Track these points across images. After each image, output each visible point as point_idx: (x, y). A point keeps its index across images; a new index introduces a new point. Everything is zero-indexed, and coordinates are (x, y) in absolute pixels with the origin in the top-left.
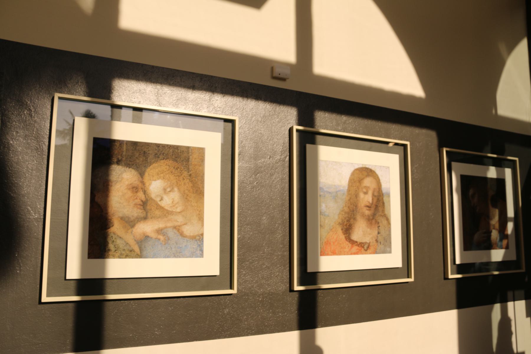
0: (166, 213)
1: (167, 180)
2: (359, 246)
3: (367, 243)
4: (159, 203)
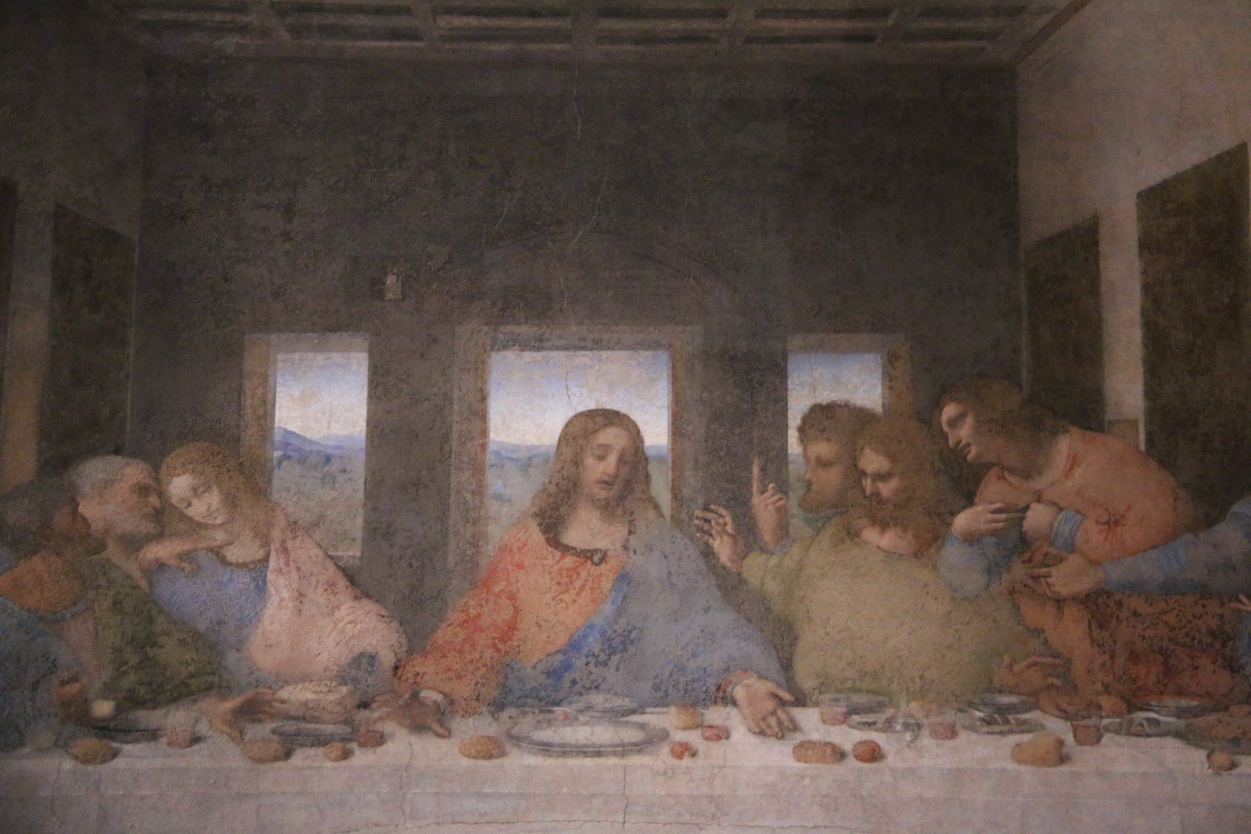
0: (196, 527)
1: (198, 474)
2: (579, 557)
3: (599, 552)
4: (185, 511)
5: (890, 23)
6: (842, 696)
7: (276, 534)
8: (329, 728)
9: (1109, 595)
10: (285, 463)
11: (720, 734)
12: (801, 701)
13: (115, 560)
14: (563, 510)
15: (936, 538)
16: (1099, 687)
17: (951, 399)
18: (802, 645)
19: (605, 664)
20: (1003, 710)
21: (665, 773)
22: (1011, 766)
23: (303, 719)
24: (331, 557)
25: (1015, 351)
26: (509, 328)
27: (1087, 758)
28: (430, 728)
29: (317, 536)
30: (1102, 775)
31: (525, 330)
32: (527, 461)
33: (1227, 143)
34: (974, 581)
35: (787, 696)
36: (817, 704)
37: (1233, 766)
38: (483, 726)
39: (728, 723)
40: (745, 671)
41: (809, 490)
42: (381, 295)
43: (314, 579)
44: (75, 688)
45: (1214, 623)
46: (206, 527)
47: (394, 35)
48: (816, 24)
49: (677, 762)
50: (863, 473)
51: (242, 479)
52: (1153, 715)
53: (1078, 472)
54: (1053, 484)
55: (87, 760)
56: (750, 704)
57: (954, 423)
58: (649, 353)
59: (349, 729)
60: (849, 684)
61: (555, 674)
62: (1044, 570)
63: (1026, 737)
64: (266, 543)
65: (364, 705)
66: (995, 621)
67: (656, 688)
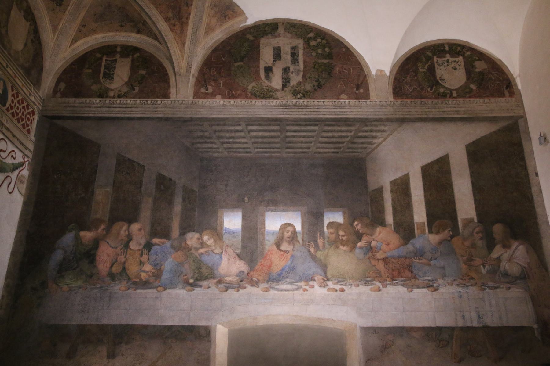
0: (209, 246)
5: (341, 150)
6: (336, 279)
7: (224, 247)
8: (235, 285)
9: (388, 258)
10: (226, 234)
11: (312, 287)
12: (328, 280)
13: (193, 252)
14: (280, 243)
15: (354, 248)
16: (386, 276)
17: (356, 221)
18: (328, 269)
19: (289, 273)
20: (368, 281)
21: (302, 294)
22: (370, 292)
23: (230, 283)
24: (235, 252)
25: (368, 211)
26: (269, 207)
27: (384, 290)
28: (255, 286)
29: (232, 248)
30: (388, 293)
31: (272, 208)
32: (273, 233)
33: (406, 173)
34: (362, 256)
35: (326, 279)
36: (331, 281)
37: (412, 291)
38: (265, 285)
39: (314, 284)
40: (317, 274)
41: (329, 239)
42: (244, 201)
43: (231, 256)
44: (185, 277)
45: (408, 263)
46: (211, 246)
47: (247, 153)
48: (327, 150)
49: (304, 292)
50: (340, 235)
51: (217, 237)
52: (397, 281)
53: (381, 235)
54: (376, 237)
55: (188, 291)
56: (318, 281)
57: (357, 225)
58: (297, 212)
59: (238, 286)
60: (338, 277)
61: (279, 275)
62: (375, 254)
63: (373, 286)
64: (222, 249)
65: (242, 281)
66: (366, 264)
67: (299, 278)
